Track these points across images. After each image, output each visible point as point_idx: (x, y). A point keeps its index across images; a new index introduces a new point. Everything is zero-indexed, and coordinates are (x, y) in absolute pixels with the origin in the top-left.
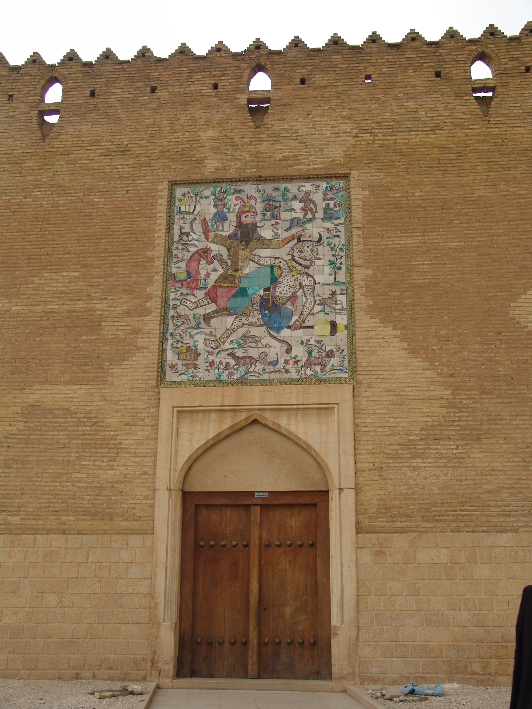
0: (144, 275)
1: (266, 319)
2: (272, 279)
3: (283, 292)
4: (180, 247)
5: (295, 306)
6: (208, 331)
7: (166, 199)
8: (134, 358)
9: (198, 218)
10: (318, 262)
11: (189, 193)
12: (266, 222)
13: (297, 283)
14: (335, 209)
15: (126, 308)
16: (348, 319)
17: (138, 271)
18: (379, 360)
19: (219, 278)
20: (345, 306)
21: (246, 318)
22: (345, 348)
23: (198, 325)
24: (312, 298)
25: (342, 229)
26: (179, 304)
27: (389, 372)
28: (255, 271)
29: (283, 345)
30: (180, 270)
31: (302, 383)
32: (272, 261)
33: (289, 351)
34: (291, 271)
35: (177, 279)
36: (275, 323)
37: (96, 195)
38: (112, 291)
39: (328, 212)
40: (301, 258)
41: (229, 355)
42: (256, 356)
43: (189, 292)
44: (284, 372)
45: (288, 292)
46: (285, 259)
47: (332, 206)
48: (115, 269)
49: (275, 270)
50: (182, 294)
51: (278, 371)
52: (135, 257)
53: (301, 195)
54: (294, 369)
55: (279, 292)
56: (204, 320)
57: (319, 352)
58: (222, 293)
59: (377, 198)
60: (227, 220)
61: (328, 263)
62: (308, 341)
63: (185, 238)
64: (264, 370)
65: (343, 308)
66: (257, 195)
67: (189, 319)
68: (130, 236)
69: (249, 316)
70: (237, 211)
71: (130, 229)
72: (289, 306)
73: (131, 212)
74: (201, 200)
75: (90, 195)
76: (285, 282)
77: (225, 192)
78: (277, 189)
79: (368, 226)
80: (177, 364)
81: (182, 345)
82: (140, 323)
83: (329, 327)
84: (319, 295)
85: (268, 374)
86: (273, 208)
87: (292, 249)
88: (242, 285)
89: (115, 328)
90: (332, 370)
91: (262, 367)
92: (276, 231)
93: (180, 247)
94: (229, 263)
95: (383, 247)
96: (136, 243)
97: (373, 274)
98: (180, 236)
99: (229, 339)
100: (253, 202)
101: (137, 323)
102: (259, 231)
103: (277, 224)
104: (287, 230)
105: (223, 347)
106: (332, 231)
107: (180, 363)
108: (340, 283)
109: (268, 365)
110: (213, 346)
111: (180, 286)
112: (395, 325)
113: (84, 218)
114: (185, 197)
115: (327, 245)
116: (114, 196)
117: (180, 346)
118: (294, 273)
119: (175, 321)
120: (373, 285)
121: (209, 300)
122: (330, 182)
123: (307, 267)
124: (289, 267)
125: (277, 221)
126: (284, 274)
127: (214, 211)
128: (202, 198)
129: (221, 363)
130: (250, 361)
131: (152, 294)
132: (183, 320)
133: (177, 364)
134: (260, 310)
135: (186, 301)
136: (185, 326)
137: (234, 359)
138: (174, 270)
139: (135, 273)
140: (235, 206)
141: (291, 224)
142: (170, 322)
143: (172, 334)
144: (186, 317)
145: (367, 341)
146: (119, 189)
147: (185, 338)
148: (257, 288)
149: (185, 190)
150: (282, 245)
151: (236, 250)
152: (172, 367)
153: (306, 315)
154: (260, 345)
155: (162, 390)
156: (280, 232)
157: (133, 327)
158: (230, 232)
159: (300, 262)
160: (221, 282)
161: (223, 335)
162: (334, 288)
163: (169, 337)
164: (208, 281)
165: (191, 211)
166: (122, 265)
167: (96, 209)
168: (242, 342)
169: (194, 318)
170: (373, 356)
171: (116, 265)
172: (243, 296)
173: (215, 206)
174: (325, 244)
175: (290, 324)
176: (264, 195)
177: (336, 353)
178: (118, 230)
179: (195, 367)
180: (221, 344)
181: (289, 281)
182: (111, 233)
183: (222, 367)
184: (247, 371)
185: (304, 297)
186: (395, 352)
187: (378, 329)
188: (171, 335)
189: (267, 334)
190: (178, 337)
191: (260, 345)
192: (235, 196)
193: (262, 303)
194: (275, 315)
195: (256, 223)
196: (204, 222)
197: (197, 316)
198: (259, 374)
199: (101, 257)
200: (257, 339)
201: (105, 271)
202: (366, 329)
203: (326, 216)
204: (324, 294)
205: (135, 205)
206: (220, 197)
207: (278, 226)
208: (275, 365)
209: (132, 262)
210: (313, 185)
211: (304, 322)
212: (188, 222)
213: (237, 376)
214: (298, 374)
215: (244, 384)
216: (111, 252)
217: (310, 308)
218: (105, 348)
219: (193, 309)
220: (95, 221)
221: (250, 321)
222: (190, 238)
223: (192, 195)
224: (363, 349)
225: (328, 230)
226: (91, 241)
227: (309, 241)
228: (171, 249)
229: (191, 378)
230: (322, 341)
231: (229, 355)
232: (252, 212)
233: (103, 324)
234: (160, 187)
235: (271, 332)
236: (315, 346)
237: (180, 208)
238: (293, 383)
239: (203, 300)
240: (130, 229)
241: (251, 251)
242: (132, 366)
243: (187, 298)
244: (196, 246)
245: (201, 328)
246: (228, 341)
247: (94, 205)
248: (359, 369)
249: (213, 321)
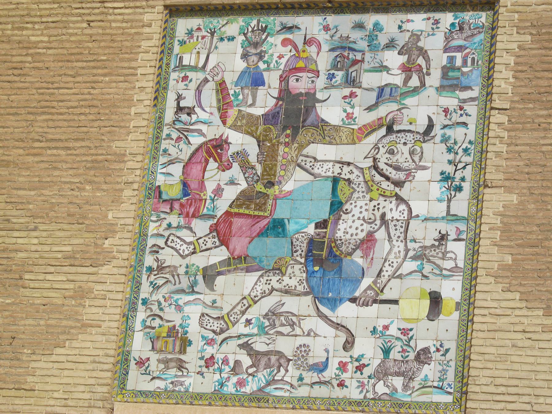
0: (104, 187)
1: (314, 281)
2: (332, 204)
3: (350, 231)
4: (175, 135)
5: (369, 260)
6: (208, 299)
7: (156, 40)
8: (75, 344)
9: (210, 79)
10: (420, 175)
11: (199, 29)
12: (333, 92)
13: (378, 214)
14: (465, 70)
15: (69, 248)
16: (464, 289)
17: (96, 179)
18: (511, 374)
19: (237, 199)
20: (461, 264)
21: (278, 278)
22: (452, 345)
23: (192, 287)
24: (402, 245)
25: (472, 109)
26: (163, 245)
27: (526, 399)
28: (303, 187)
29: (339, 333)
30: (171, 180)
31: (366, 409)
32: (337, 170)
33: (348, 345)
34: (369, 190)
35: (164, 197)
36: (329, 291)
37: (33, 29)
38: (47, 214)
39: (450, 74)
40: (391, 166)
41: (241, 346)
42: (288, 352)
43: (182, 221)
44: (335, 385)
45: (359, 231)
46: (361, 165)
47: (459, 62)
48: (56, 173)
49: (339, 187)
50: (169, 226)
51: (325, 383)
52: (92, 151)
53: (402, 39)
54: (354, 381)
55: (342, 230)
56: (204, 277)
57: (404, 351)
58: (241, 228)
59: (545, 48)
60: (263, 84)
61: (439, 178)
62: (386, 328)
63: (184, 117)
64: (301, 379)
65: (456, 266)
66: (322, 37)
67: (178, 275)
68: (87, 111)
69: (283, 275)
70: (282, 67)
71: (87, 97)
72: (358, 258)
73: (92, 64)
74: (221, 45)
75: (23, 29)
76: (356, 211)
77: (264, 30)
78: (360, 26)
79: (521, 106)
80: (148, 359)
81: (161, 323)
82: (92, 278)
83: (427, 303)
84: (414, 241)
85: (308, 388)
86: (349, 63)
87: (376, 147)
88: (278, 215)
89: (48, 285)
90: (423, 387)
91: (297, 373)
92: (349, 110)
93: (175, 135)
94: (259, 169)
95: (544, 149)
96: (96, 124)
97: (521, 203)
98: (176, 113)
99: (245, 317)
100: (313, 49)
101: (85, 278)
102: (319, 110)
103: (352, 95)
104: (370, 109)
105: (233, 331)
106: (454, 114)
107: (154, 357)
108: (456, 218)
109: (309, 370)
110: (215, 328)
111: (168, 211)
112: (548, 307)
113: (10, 72)
114: (192, 37)
115: (442, 142)
116: (64, 31)
117: (157, 326)
118: (375, 194)
119: (152, 278)
120: (516, 224)
121: (216, 240)
122: (460, 14)
123: (399, 184)
124: (366, 182)
125: (354, 90)
126: (355, 195)
127: (241, 65)
128: (222, 39)
129: (225, 361)
130: (278, 360)
131: (117, 224)
132: (167, 276)
133: (148, 359)
134: (306, 265)
135: (176, 239)
136: (169, 287)
137: (249, 355)
138: (160, 180)
139: (90, 182)
140: (281, 57)
141: (378, 98)
142: (145, 277)
143: (145, 302)
144: (173, 269)
145: (491, 335)
146: (75, 19)
147: (167, 310)
148: (304, 221)
149: (194, 22)
150: (358, 138)
151: (273, 145)
152: (141, 363)
153: (386, 277)
154: (298, 331)
155: (117, 406)
156: (357, 112)
157: (78, 284)
158: (267, 109)
159: (388, 173)
160: (240, 206)
161: (234, 308)
162: (443, 227)
163: (141, 307)
164: (218, 203)
165: (201, 65)
166: (69, 166)
167: (31, 55)
168: (267, 323)
169: (187, 273)
170: (499, 366)
171: (59, 165)
172: (277, 236)
173: (245, 56)
174: (438, 139)
175: (357, 294)
176: (336, 38)
177: (433, 355)
178: (68, 98)
179: (181, 365)
180: (230, 325)
181: (363, 210)
182: (55, 104)
183: (227, 369)
184: (271, 378)
185: (387, 242)
186: (543, 361)
187: (518, 312)
188: (143, 304)
189: (313, 312)
190: (155, 308)
191: (298, 331)
192: (282, 37)
193: (309, 251)
194: (330, 275)
195: (315, 94)
196: (222, 87)
197: (193, 270)
198: (292, 385)
199: (34, 148)
200: (294, 319)
201: (38, 176)
202: (492, 311)
203: (446, 83)
204: (424, 239)
205: (100, 51)
206: (254, 40)
207: (355, 101)
208: (322, 371)
209: (86, 161)
210: (429, 19)
211: (382, 291)
212: (193, 86)
213: (251, 387)
214: (361, 392)
215: (262, 404)
216: (52, 140)
217: (395, 265)
218: (27, 322)
219: (187, 256)
220: (28, 79)
221: (284, 283)
222: (194, 117)
223: (205, 34)
224: (483, 350)
225: (446, 111)
226: (18, 118)
227: (409, 131)
228: (157, 138)
229: (171, 386)
230: (411, 330)
231: (241, 346)
232: (309, 71)
233: (27, 276)
234: (147, 18)
235: (321, 308)
236: (398, 339)
237: (181, 59)
238: (349, 408)
239: (207, 239)
240: (87, 97)
241: (302, 147)
242: (70, 358)
243: (179, 234)
244: (204, 135)
245: (198, 293)
246: (243, 320)
247: (30, 48)
248: (471, 388)
249: (220, 280)
